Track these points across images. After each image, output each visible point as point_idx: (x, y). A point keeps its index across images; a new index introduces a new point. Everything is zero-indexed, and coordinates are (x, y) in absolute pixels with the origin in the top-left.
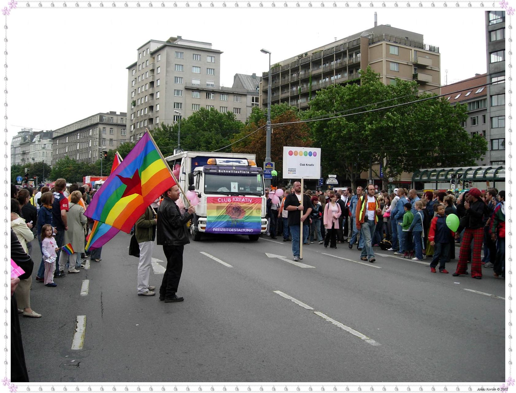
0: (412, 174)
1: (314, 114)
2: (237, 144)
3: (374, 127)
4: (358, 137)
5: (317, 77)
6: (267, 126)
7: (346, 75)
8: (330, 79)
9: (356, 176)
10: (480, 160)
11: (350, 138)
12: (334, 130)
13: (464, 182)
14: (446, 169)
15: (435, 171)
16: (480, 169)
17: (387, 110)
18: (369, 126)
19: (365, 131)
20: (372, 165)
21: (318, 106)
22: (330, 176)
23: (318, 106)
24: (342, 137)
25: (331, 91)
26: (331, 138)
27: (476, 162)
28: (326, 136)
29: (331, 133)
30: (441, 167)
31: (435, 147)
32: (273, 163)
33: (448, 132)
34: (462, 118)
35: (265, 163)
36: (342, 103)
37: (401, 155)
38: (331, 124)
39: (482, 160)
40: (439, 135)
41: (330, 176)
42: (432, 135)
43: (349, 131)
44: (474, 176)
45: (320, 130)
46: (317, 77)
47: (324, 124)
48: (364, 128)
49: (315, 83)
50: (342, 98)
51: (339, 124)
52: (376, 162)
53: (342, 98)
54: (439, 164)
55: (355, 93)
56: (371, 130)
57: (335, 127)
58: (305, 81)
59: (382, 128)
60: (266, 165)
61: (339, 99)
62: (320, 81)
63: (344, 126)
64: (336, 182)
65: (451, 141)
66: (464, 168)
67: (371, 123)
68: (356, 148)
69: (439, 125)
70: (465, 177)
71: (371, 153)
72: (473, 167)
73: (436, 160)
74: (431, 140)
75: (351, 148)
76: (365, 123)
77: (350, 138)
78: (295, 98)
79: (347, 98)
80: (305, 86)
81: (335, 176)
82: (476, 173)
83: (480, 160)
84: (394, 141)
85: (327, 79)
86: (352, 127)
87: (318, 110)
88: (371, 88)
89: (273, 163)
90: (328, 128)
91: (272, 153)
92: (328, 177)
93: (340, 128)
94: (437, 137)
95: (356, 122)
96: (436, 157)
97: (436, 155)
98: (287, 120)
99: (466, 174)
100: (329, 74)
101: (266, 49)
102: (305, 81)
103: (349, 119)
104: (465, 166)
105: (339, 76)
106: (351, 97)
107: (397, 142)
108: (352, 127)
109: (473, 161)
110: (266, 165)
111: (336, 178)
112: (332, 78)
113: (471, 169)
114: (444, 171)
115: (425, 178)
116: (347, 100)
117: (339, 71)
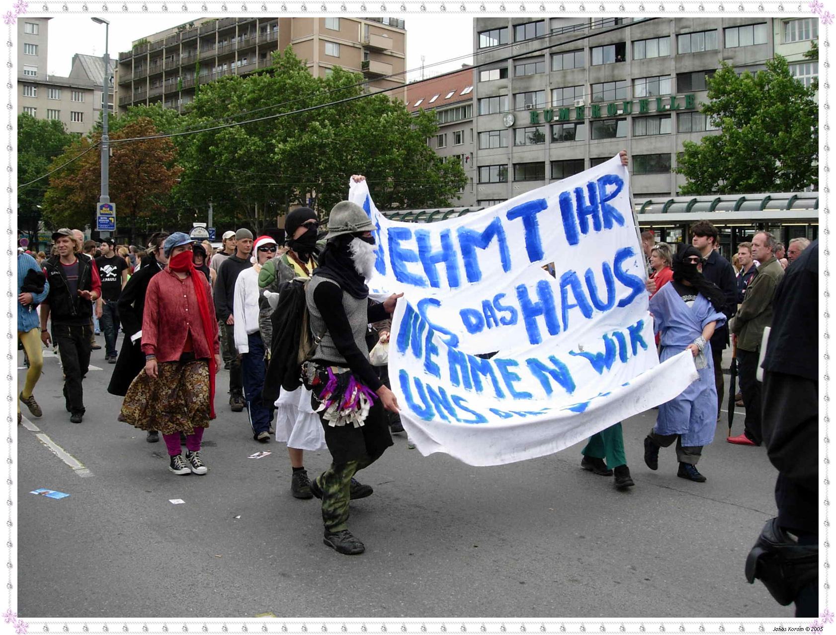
1: (194, 123)
2: (59, 172)
3: (288, 147)
4: (264, 161)
5: (208, 64)
6: (101, 143)
7: (256, 60)
8: (230, 66)
9: (264, 225)
10: (456, 199)
11: (252, 163)
12: (226, 148)
14: (401, 212)
17: (312, 118)
18: (281, 146)
19: (275, 153)
20: (289, 206)
21: (201, 110)
22: (195, 225)
23: (201, 110)
24: (238, 160)
25: (224, 87)
26: (220, 162)
27: (450, 201)
28: (214, 159)
29: (221, 155)
30: (398, 208)
31: (385, 178)
32: (113, 205)
33: (408, 154)
34: (427, 131)
35: (99, 205)
36: (241, 106)
37: (335, 191)
38: (222, 140)
39: (459, 198)
40: (391, 160)
41: (195, 225)
42: (379, 159)
43: (249, 150)
45: (203, 149)
46: (208, 64)
47: (210, 139)
48: (271, 148)
49: (204, 73)
50: (240, 97)
51: (233, 139)
52: (296, 203)
54: (395, 205)
56: (283, 152)
57: (226, 143)
58: (189, 68)
59: (301, 148)
60: (101, 209)
61: (235, 98)
62: (214, 70)
63: (241, 142)
64: (205, 234)
65: (413, 169)
66: (427, 211)
67: (285, 141)
68: (264, 179)
69: (392, 144)
71: (284, 188)
72: (441, 210)
74: (378, 167)
75: (250, 179)
76: (274, 141)
77: (252, 163)
78: (172, 96)
80: (189, 77)
81: (204, 225)
83: (456, 199)
84: (321, 167)
85: (225, 67)
86: (254, 144)
87: (201, 116)
88: (289, 81)
89: (113, 205)
90: (218, 147)
91: (111, 187)
92: (193, 227)
93: (235, 144)
94: (391, 162)
95: (262, 136)
96: (392, 193)
97: (389, 190)
98: (142, 133)
100: (228, 58)
102: (189, 68)
103: (251, 130)
104: (431, 208)
105: (244, 62)
106: (255, 95)
107: (326, 169)
108: (254, 144)
109: (446, 199)
110: (101, 209)
111: (207, 228)
112: (233, 65)
116: (249, 101)
117: (244, 53)
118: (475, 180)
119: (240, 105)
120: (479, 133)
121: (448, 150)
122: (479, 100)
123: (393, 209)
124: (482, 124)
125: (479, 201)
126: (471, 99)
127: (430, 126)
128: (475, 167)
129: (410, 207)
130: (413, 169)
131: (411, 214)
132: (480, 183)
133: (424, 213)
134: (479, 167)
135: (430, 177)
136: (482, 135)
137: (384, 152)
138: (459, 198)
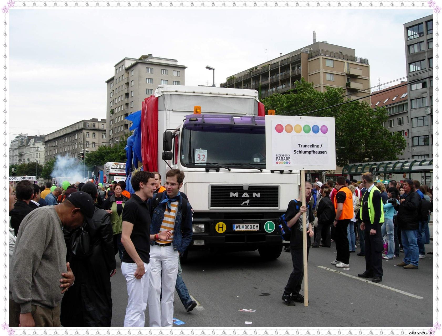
0: (343, 168)
7: (290, 84)
8: (277, 88)
13: (385, 174)
14: (370, 163)
15: (361, 165)
16: (399, 162)
27: (397, 156)
30: (368, 161)
31: (360, 144)
39: (402, 154)
44: (393, 169)
50: (282, 105)
53: (282, 105)
54: (366, 159)
55: (293, 101)
61: (279, 105)
62: (268, 91)
66: (385, 162)
70: (377, 170)
72: (392, 162)
73: (364, 156)
79: (285, 105)
82: (394, 166)
83: (400, 155)
85: (274, 89)
96: (364, 153)
97: (363, 151)
99: (386, 167)
100: (275, 84)
101: (210, 66)
105: (284, 86)
106: (289, 104)
112: (278, 88)
113: (391, 163)
114: (368, 164)
115: (353, 171)
116: (286, 107)
117: (284, 81)
118: (411, 145)
119: (282, 109)
120: (412, 119)
121: (395, 128)
122: (411, 100)
123: (365, 161)
124: (413, 114)
125: (413, 156)
126: (407, 100)
127: (383, 116)
128: (410, 137)
129: (375, 160)
130: (376, 139)
131: (375, 164)
132: (413, 146)
133: (383, 163)
134: (413, 137)
135: (385, 143)
136: (414, 120)
137: (359, 131)
138: (402, 154)
